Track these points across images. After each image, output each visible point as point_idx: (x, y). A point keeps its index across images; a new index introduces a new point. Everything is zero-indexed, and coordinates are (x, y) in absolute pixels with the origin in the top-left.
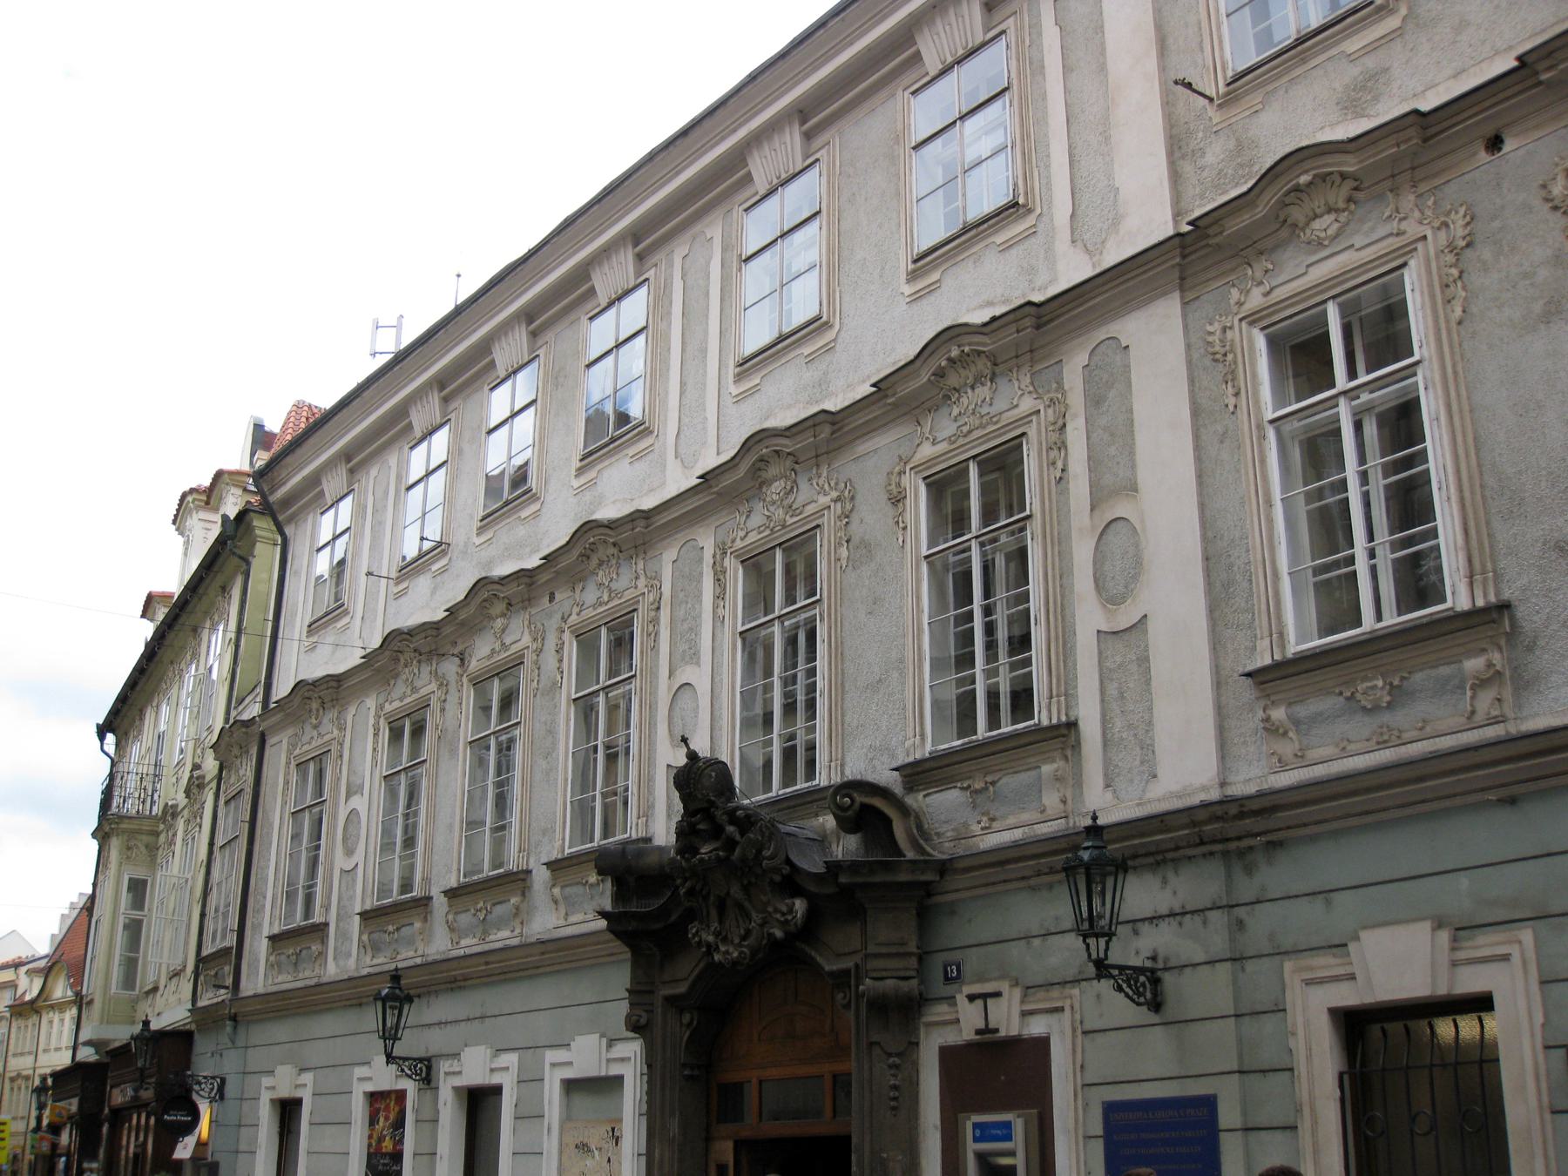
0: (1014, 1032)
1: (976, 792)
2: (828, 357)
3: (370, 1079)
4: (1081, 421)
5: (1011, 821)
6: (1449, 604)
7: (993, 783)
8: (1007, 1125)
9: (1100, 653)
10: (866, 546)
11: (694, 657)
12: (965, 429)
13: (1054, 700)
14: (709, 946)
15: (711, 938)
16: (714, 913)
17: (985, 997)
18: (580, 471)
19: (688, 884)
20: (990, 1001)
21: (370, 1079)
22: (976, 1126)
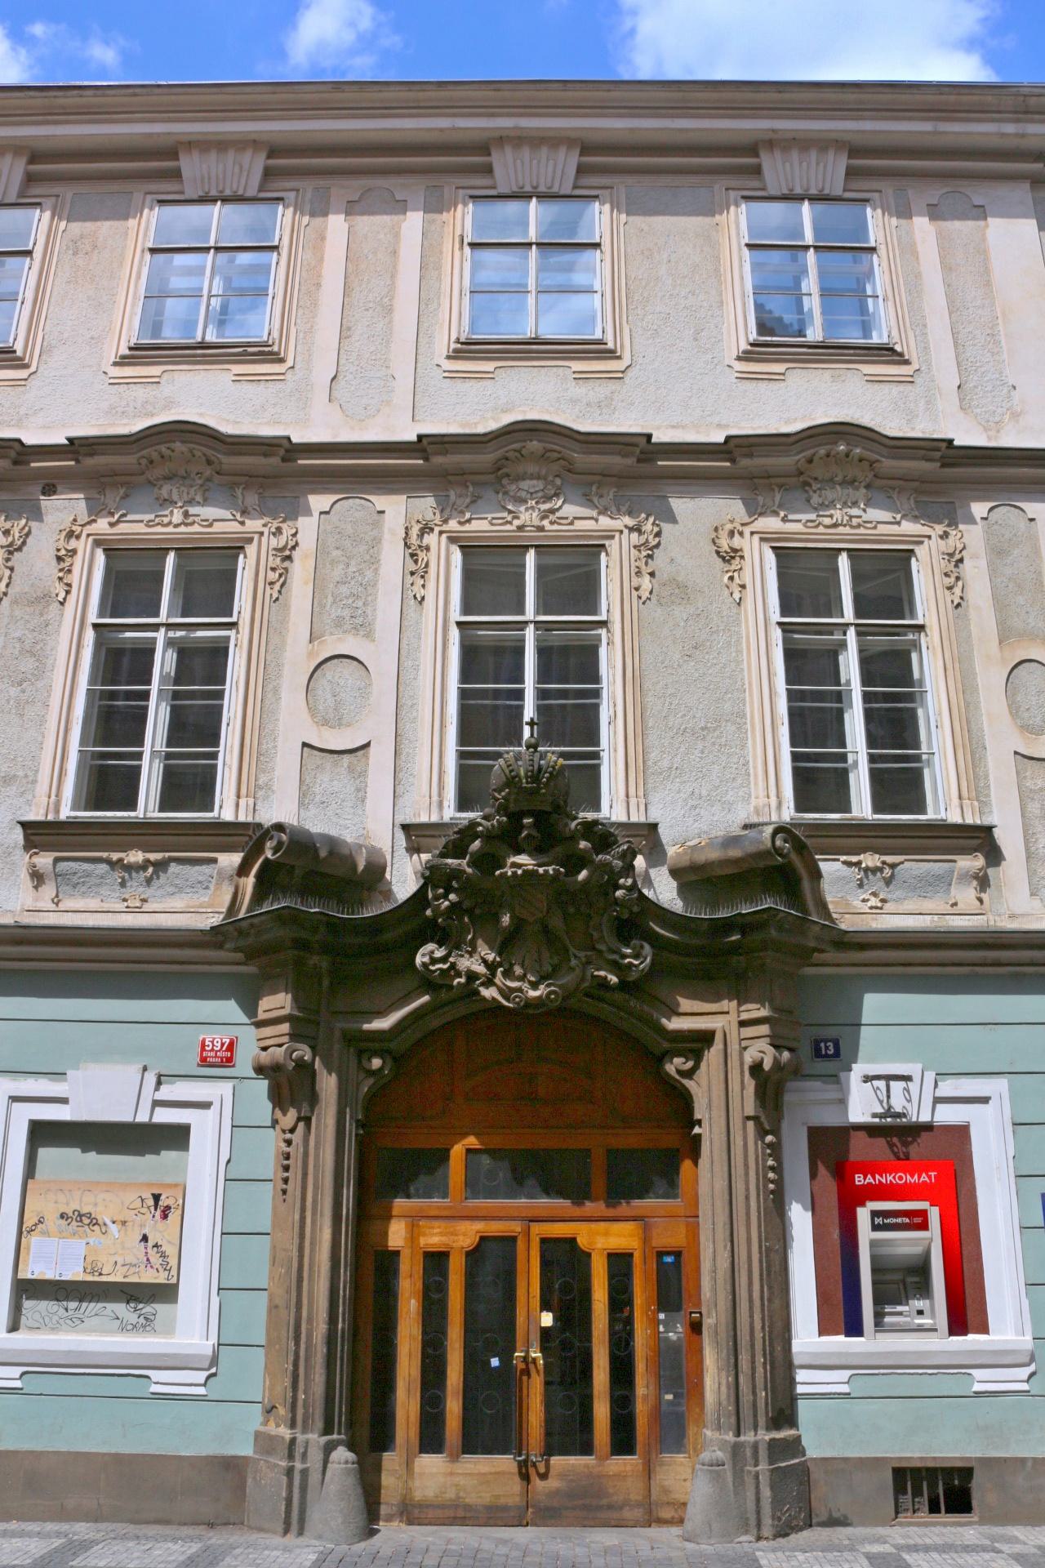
0: (925, 1117)
1: (867, 870)
2: (612, 386)
3: (64, 1101)
4: (983, 563)
5: (909, 906)
6: (215, 814)
7: (893, 866)
8: (923, 1214)
9: (1018, 773)
10: (681, 591)
11: (364, 628)
12: (827, 521)
13: (966, 802)
14: (472, 976)
15: (481, 969)
17: (889, 1078)
18: (123, 361)
19: (452, 897)
20: (892, 1083)
21: (64, 1101)
22: (875, 1214)
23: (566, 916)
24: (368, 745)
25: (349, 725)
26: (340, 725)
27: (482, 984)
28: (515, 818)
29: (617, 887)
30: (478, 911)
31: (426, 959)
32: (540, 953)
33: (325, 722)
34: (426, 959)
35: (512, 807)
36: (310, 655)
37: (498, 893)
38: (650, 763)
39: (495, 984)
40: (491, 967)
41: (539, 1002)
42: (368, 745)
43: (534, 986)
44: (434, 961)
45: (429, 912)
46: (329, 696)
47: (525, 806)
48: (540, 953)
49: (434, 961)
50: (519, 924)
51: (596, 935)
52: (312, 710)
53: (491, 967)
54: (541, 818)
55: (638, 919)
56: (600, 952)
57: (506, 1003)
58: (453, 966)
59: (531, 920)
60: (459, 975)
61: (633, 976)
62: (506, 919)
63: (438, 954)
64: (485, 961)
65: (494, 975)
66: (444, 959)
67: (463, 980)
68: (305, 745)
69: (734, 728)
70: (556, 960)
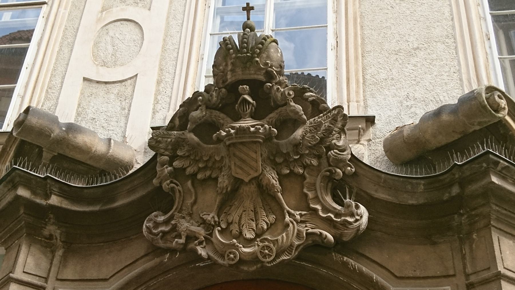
14: (191, 237)
16: (210, 198)
19: (176, 164)
23: (281, 178)
24: (137, 75)
25: (122, 65)
26: (115, 65)
27: (200, 243)
28: (233, 89)
29: (330, 148)
30: (199, 176)
31: (151, 225)
32: (256, 213)
33: (104, 64)
34: (151, 225)
35: (230, 78)
36: (99, 20)
37: (217, 158)
38: (368, 77)
39: (212, 242)
40: (209, 227)
41: (254, 259)
42: (137, 75)
43: (249, 242)
44: (157, 225)
45: (155, 181)
46: (110, 48)
47: (240, 75)
48: (256, 213)
49: (157, 225)
50: (238, 183)
51: (310, 195)
52: (95, 57)
53: (209, 227)
54: (257, 88)
55: (349, 181)
56: (316, 210)
57: (220, 261)
58: (174, 228)
59: (247, 180)
60: (179, 236)
61: (348, 235)
62: (224, 182)
63: (161, 219)
64: (203, 223)
65: (211, 235)
66: (166, 222)
67: (182, 241)
68: (85, 79)
69: (443, 46)
70: (272, 218)
